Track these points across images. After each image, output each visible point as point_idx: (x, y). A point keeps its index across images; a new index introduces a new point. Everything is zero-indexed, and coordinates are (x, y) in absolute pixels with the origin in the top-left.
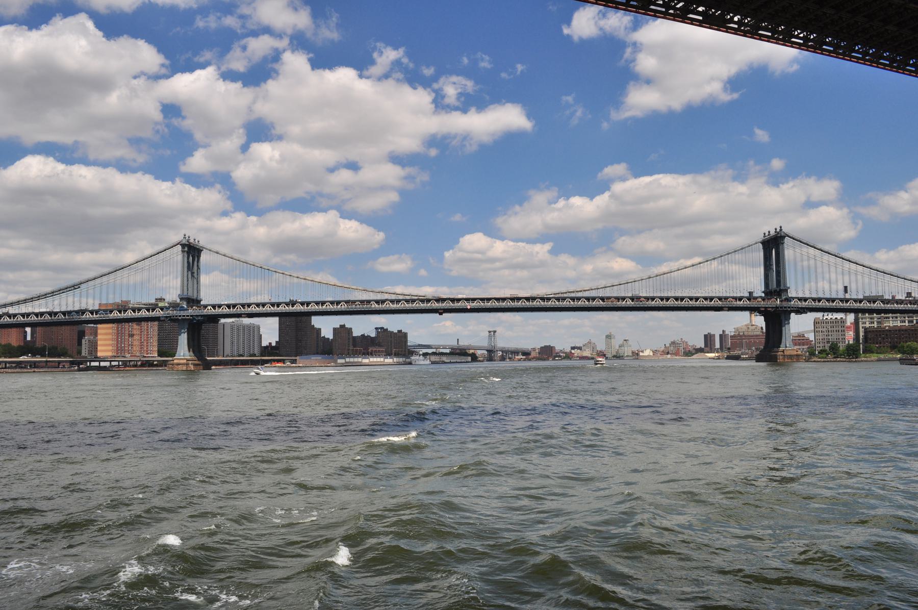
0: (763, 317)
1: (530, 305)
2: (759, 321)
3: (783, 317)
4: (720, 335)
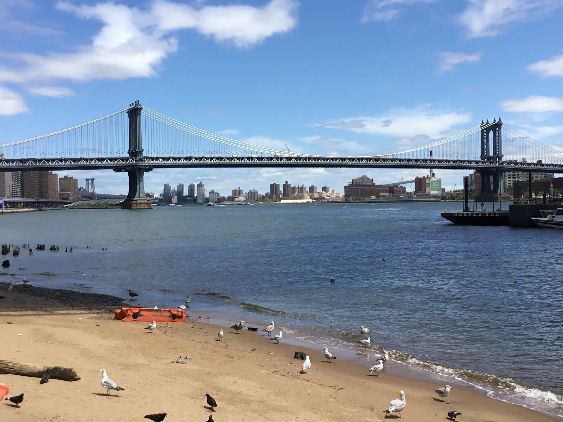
0: (127, 173)
2: (125, 175)
3: (138, 174)
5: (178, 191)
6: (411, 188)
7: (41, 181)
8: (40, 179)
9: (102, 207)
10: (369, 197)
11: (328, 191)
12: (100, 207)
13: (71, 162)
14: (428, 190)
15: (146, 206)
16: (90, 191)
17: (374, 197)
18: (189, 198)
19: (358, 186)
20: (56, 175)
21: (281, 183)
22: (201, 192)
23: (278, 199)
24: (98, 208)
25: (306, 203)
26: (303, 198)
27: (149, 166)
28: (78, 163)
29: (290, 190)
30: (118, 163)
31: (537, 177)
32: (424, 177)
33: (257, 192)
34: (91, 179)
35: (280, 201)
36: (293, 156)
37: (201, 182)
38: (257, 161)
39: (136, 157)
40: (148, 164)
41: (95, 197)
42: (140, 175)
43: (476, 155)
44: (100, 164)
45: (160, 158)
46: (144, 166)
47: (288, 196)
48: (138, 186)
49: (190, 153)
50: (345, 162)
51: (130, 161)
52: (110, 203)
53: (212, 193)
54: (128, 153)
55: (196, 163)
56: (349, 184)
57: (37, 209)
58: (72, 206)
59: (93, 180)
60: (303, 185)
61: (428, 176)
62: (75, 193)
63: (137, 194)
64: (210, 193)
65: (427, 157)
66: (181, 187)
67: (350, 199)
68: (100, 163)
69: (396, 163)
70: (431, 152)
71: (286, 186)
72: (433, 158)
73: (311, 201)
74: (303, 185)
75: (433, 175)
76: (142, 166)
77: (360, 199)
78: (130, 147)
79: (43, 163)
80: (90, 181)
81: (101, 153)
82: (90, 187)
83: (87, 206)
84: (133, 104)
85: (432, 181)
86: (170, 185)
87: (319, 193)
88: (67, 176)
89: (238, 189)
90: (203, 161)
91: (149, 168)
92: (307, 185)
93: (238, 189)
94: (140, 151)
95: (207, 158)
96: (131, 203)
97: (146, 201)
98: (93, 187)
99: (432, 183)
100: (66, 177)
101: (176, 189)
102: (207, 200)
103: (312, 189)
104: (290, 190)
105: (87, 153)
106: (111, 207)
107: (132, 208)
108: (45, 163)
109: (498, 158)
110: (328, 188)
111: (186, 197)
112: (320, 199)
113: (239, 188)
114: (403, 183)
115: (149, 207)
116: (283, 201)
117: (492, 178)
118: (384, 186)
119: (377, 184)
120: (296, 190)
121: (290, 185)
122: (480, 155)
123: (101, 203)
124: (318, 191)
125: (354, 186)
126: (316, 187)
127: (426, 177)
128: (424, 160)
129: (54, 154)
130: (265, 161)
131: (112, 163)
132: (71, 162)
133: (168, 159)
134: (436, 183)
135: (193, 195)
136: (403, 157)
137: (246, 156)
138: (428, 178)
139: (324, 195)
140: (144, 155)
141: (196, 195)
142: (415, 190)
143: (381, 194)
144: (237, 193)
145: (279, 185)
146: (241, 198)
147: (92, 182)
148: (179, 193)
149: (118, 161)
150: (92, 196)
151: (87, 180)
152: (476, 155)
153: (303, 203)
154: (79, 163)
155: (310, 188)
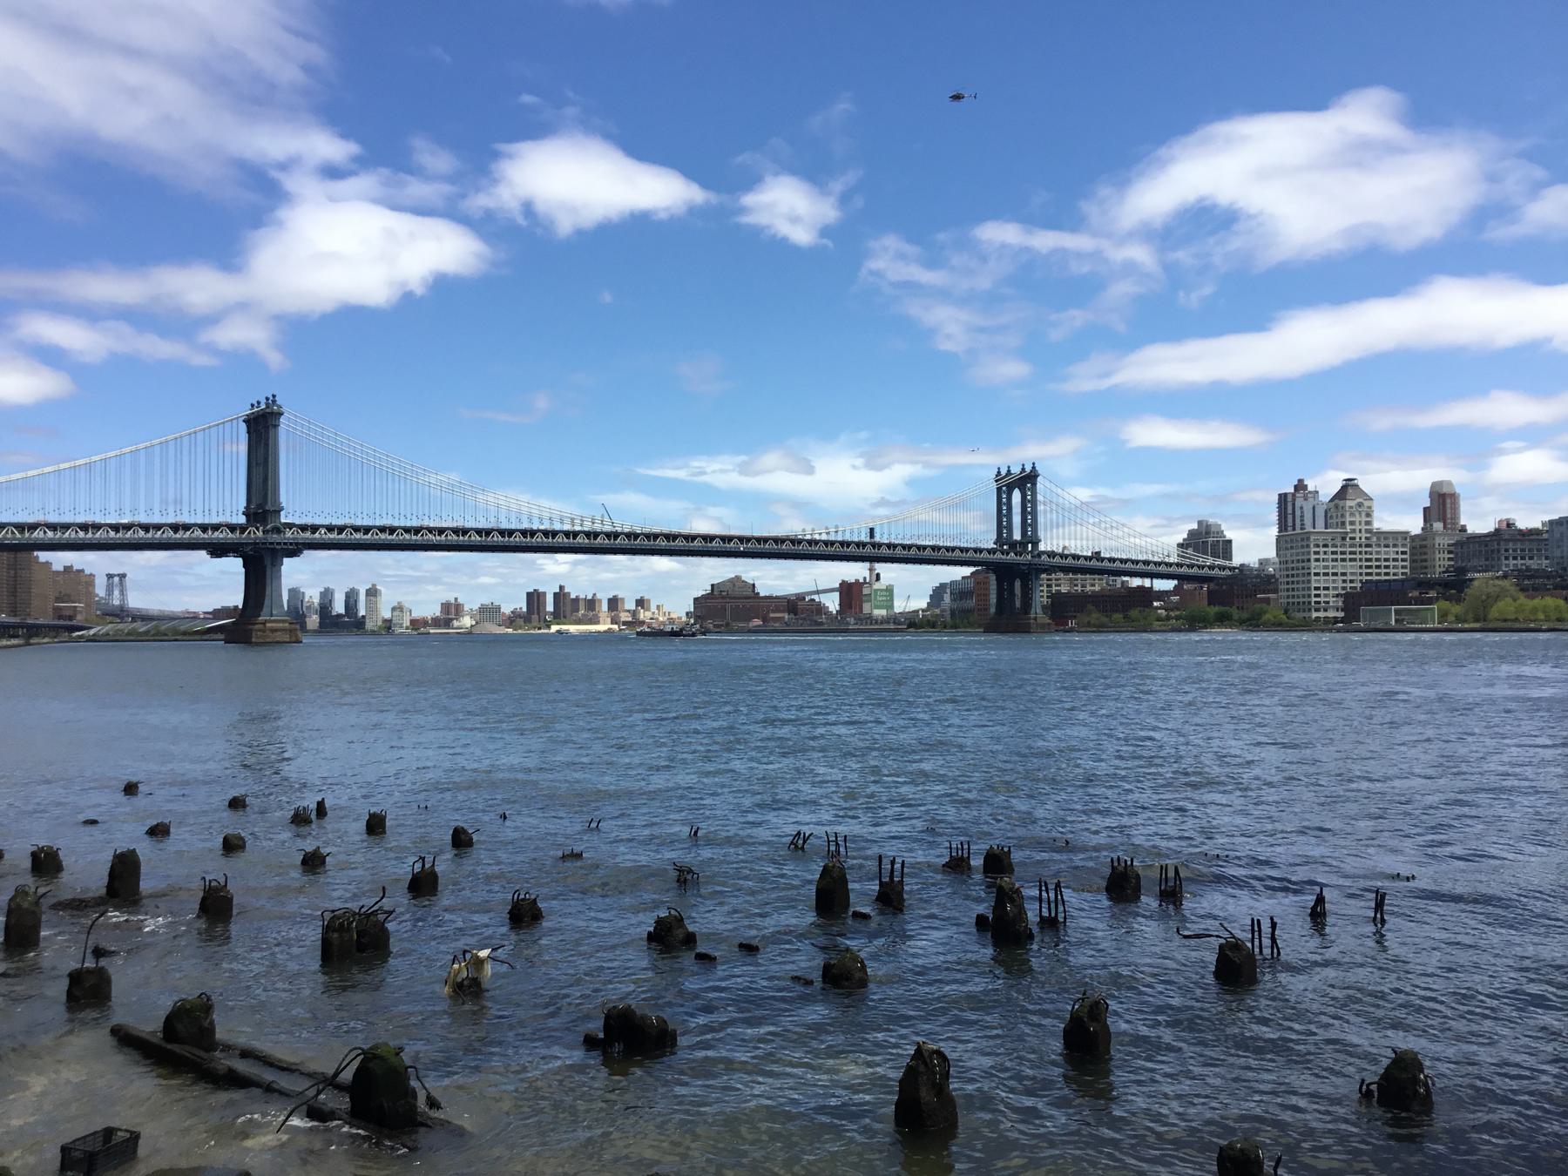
0: (240, 561)
1: (411, 540)
2: (234, 566)
3: (268, 562)
4: (555, 594)
5: (320, 604)
6: (832, 603)
7: (15, 577)
8: (12, 572)
9: (166, 638)
10: (750, 620)
11: (648, 610)
12: (134, 637)
13: (45, 532)
14: (866, 608)
15: (286, 638)
16: (116, 602)
17: (757, 622)
18: (346, 619)
19: (723, 598)
20: (48, 564)
21: (550, 593)
22: (372, 608)
23: (542, 623)
24: (155, 641)
25: (605, 632)
26: (598, 623)
27: (297, 544)
28: (64, 533)
29: (568, 608)
30: (165, 536)
31: (1093, 585)
32: (857, 581)
33: (499, 608)
34: (119, 575)
35: (549, 627)
36: (619, 530)
37: (374, 585)
38: (476, 538)
39: (264, 522)
40: (294, 539)
41: (128, 616)
42: (273, 565)
43: (984, 536)
44: (119, 539)
45: (323, 526)
46: (285, 544)
47: (565, 617)
48: (268, 592)
49: (365, 517)
50: (390, 537)
51: (249, 533)
52: (182, 628)
53: (399, 608)
54: (244, 513)
55: (329, 539)
56: (704, 593)
57: (21, 641)
58: (94, 635)
59: (123, 576)
60: (595, 595)
61: (865, 578)
62: (88, 605)
63: (266, 610)
64: (394, 609)
65: (865, 538)
66: (327, 595)
67: (709, 624)
68: (120, 535)
69: (767, 546)
70: (872, 530)
71: (560, 596)
72: (877, 539)
73: (615, 627)
74: (595, 595)
75: (878, 577)
76: (279, 544)
77: (728, 624)
78: (249, 501)
79: (7, 532)
80: (116, 579)
81: (136, 512)
82: (116, 593)
83: (128, 634)
84: (259, 403)
85: (876, 590)
86: (302, 590)
87: (629, 611)
88: (72, 566)
89: (453, 601)
90: (372, 535)
91: (295, 550)
92: (604, 597)
93: (453, 601)
94: (275, 511)
95: (430, 530)
96: (251, 630)
97: (287, 625)
98: (122, 592)
99: (876, 596)
100: (68, 569)
101: (316, 600)
102: (388, 625)
103: (614, 603)
104: (568, 608)
105: (73, 512)
106: (185, 638)
107: (253, 640)
108: (13, 533)
109: (1030, 545)
110: (649, 601)
111: (339, 616)
112: (635, 622)
113: (456, 599)
114: (818, 592)
115: (294, 639)
116: (554, 628)
117: (1018, 584)
118: (777, 597)
119: (762, 594)
120: (582, 605)
121: (569, 593)
122: (994, 537)
123: (163, 628)
124: (627, 607)
125: (717, 598)
126: (623, 599)
127: (861, 581)
128: (858, 544)
129: (20, 512)
130: (517, 539)
131: (149, 535)
132: (45, 532)
133: (341, 529)
134: (884, 593)
135: (356, 613)
136: (848, 538)
137: (377, 524)
138: (865, 583)
139: (643, 615)
140: (283, 520)
141: (362, 612)
142: (838, 608)
143: (772, 615)
144: (451, 610)
145: (544, 593)
146: (467, 621)
147: (121, 580)
148: (325, 608)
149: (163, 532)
150: (121, 613)
151: (110, 576)
152: (979, 532)
153: (599, 632)
154: (98, 535)
155: (610, 600)
